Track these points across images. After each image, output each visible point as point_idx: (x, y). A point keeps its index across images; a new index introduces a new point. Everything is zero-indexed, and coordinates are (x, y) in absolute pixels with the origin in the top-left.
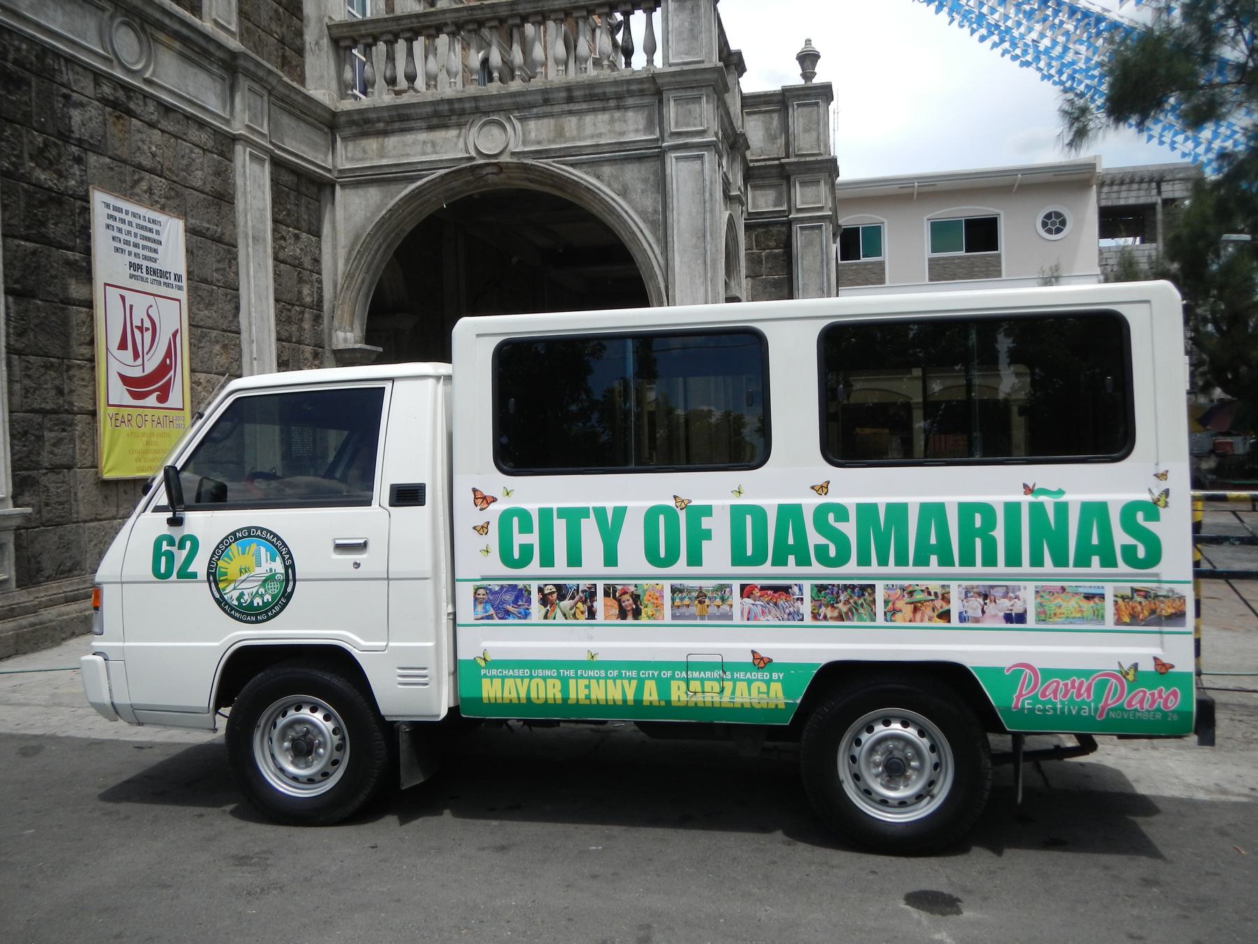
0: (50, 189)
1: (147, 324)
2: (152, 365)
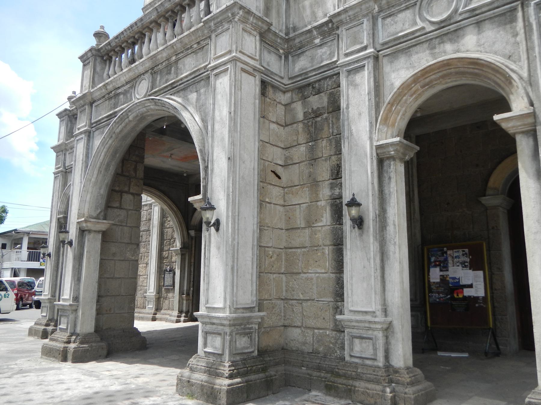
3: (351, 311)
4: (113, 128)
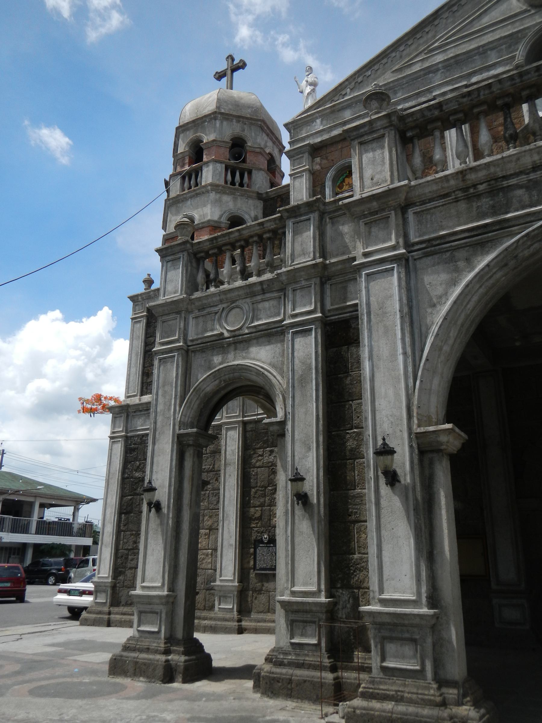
0: (140, 478)
4: (516, 249)
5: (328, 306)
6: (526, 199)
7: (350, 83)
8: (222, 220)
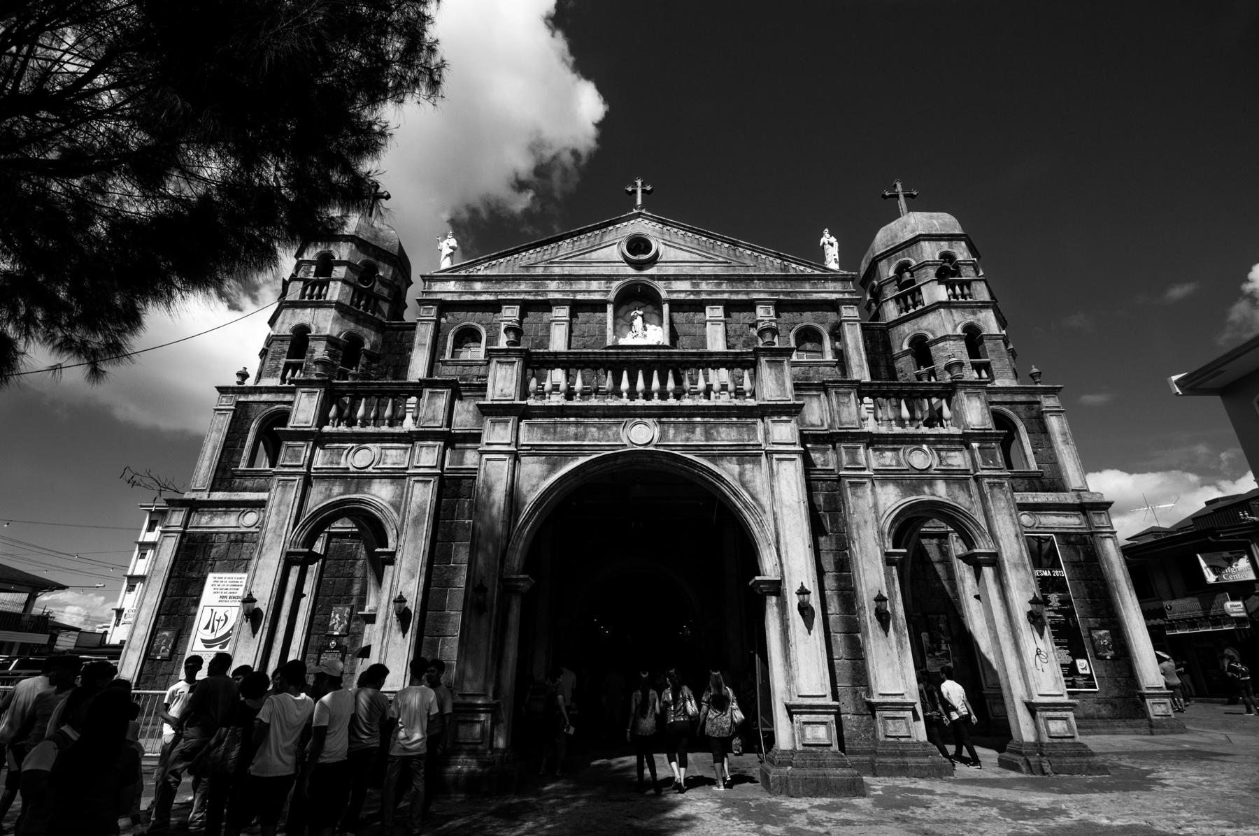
1: (224, 618)
2: (220, 634)
3: (880, 694)
5: (446, 465)
6: (596, 435)
7: (485, 262)
8: (341, 337)
